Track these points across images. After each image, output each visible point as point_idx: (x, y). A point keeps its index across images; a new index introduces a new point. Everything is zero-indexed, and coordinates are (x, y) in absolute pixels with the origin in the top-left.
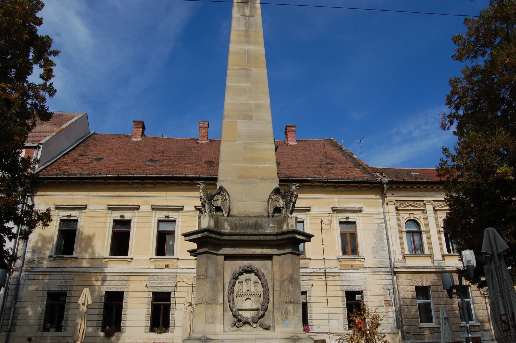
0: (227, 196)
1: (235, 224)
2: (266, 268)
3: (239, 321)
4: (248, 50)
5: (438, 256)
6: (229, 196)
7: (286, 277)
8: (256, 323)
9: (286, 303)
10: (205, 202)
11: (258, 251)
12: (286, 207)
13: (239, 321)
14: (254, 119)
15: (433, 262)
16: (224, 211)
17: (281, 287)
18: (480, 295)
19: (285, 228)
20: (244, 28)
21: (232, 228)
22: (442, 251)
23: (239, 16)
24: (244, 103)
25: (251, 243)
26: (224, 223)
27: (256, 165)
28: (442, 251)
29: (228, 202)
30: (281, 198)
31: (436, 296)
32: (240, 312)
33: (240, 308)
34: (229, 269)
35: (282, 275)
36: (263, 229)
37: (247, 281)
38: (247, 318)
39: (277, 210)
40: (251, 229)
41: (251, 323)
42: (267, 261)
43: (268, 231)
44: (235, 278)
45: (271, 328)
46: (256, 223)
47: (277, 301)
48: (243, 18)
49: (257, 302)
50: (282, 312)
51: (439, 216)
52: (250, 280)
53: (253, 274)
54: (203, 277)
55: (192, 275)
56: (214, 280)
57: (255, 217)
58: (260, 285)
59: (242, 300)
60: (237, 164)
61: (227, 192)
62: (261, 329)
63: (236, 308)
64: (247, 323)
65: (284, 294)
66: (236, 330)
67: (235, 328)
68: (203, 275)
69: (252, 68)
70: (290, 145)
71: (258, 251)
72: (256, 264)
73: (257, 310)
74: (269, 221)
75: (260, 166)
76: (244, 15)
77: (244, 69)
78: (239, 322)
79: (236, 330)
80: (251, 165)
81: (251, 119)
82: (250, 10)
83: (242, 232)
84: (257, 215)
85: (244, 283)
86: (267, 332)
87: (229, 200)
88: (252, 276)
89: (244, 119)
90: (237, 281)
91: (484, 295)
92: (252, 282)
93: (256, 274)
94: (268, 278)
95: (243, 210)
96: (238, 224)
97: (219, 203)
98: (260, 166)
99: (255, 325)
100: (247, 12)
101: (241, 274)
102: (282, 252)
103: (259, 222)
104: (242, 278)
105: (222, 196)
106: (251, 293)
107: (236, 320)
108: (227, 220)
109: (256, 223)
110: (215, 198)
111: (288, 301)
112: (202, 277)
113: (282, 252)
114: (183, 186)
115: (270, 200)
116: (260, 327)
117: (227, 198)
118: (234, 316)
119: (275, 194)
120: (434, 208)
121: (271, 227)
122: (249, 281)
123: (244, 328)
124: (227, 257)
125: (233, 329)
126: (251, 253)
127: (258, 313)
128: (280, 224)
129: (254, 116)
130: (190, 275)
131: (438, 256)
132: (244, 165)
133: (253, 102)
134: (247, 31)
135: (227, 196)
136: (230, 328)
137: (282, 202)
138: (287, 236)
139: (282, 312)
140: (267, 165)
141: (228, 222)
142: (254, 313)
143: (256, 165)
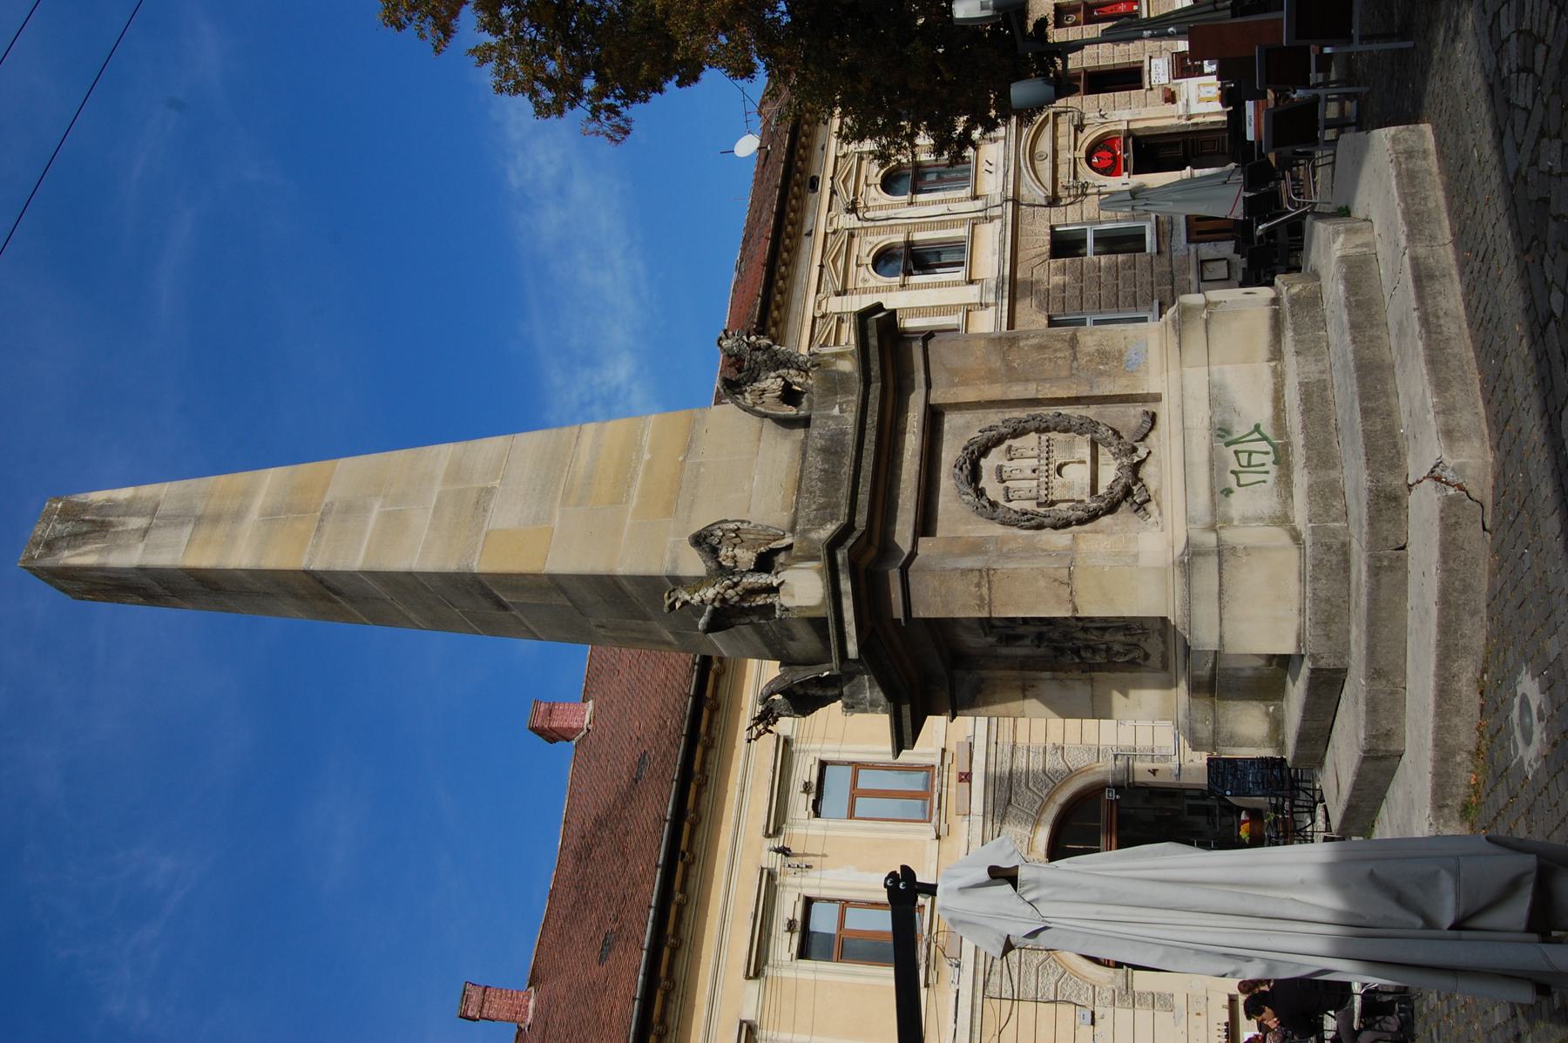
0: (725, 526)
1: (822, 507)
2: (968, 426)
3: (1128, 492)
4: (262, 515)
5: (971, 294)
6: (726, 521)
8: (1134, 450)
9: (1075, 358)
10: (736, 585)
11: (912, 442)
12: (785, 366)
13: (1128, 492)
15: (983, 306)
16: (773, 545)
17: (1027, 380)
18: (1077, 206)
19: (847, 366)
20: (187, 531)
21: (833, 517)
22: (956, 284)
23: (141, 546)
25: (884, 459)
26: (812, 541)
27: (641, 469)
28: (956, 284)
29: (745, 526)
30: (756, 385)
31: (1076, 304)
32: (1102, 490)
35: (992, 377)
36: (844, 433)
39: (789, 395)
40: (841, 465)
41: (1136, 459)
42: (946, 426)
43: (851, 418)
45: (1151, 407)
46: (824, 451)
47: (1069, 388)
48: (154, 536)
49: (1070, 446)
50: (1101, 374)
51: (860, 285)
52: (1000, 469)
53: (983, 462)
54: (984, 582)
55: (979, 1001)
57: (804, 455)
58: (1016, 443)
60: (629, 521)
62: (1152, 435)
63: (1088, 500)
64: (1136, 467)
65: (1048, 366)
66: (1158, 505)
67: (1151, 507)
68: (978, 585)
69: (327, 500)
70: (593, 720)
71: (912, 442)
72: (950, 453)
73: (1094, 445)
74: (822, 416)
75: (647, 456)
76: (145, 532)
77: (322, 520)
78: (1129, 496)
79: (1158, 505)
80: (638, 483)
82: (133, 515)
83: (845, 490)
84: (798, 455)
86: (1162, 420)
87: (743, 522)
89: (485, 510)
90: (1002, 501)
91: (1076, 196)
92: (1007, 463)
93: (984, 451)
94: (995, 418)
95: (779, 497)
96: (822, 500)
97: (746, 557)
98: (647, 456)
99: (1142, 452)
100: (137, 523)
101: (980, 493)
102: (920, 377)
103: (820, 443)
106: (1044, 462)
107: (1124, 505)
108: (805, 531)
109: (824, 451)
112: (985, 591)
113: (920, 377)
114: (671, 1020)
116: (1148, 440)
117: (732, 526)
118: (1112, 509)
119: (742, 393)
120: (838, 294)
121: (841, 411)
123: (1152, 484)
124: (926, 524)
125: (1156, 513)
126: (917, 460)
128: (834, 385)
129: (482, 485)
130: (979, 1008)
131: (971, 294)
132: (634, 502)
133: (437, 488)
134: (199, 520)
135: (725, 526)
137: (769, 381)
138: (873, 342)
139: (1101, 374)
140: (647, 439)
141: (810, 530)
142: (1105, 455)
143: (641, 469)
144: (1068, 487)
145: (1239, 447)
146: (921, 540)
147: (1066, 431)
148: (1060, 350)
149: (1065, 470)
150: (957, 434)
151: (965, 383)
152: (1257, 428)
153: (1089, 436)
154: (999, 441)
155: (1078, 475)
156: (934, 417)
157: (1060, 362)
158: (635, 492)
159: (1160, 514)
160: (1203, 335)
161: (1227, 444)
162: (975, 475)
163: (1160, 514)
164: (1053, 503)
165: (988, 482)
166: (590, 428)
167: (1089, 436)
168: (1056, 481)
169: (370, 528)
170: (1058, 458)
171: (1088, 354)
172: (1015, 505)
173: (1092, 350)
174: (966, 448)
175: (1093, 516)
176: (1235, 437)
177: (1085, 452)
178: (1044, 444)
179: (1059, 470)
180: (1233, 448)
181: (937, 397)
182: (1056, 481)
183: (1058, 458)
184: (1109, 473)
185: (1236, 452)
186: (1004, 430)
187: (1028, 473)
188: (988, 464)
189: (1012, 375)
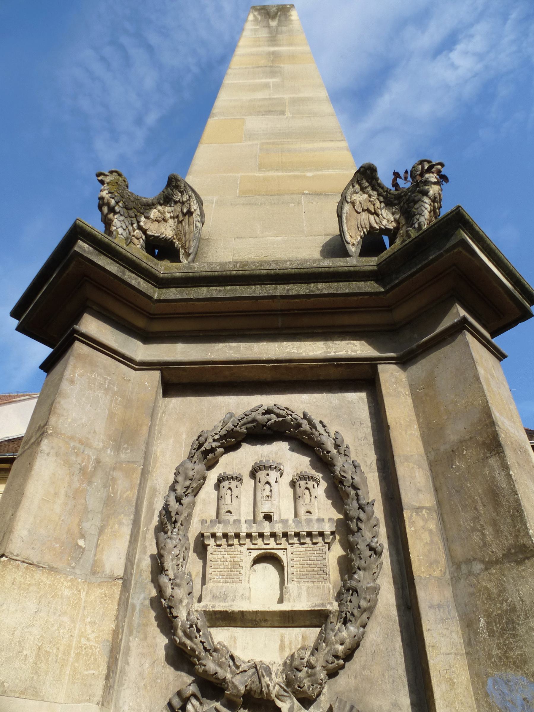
6: (200, 203)
7: (455, 431)
9: (489, 565)
32: (220, 635)
33: (220, 606)
35: (431, 433)
38: (258, 670)
47: (432, 564)
58: (320, 489)
59: (235, 565)
60: (239, 175)
61: (193, 191)
73: (317, 618)
81: (283, 113)
82: (279, 22)
87: (202, 215)
97: (167, 231)
98: (310, 174)
105: (178, 208)
106: (279, 529)
107: (185, 681)
110: (154, 213)
111: (497, 549)
115: (347, 208)
117: (194, 206)
118: (181, 657)
122: (274, 475)
124: (178, 382)
127: (323, 638)
144: (233, 572)
146: (157, 374)
147: (347, 567)
148: (498, 532)
149: (268, 570)
150: (340, 415)
151: (418, 402)
153: (334, 606)
154: (323, 462)
155: (259, 590)
156: (360, 377)
157: (476, 537)
162: (260, 432)
164: (201, 549)
165: (249, 454)
166: (344, 144)
167: (334, 606)
168: (245, 554)
170: (292, 554)
171: (502, 591)
173: (513, 597)
174: (305, 416)
175: (166, 620)
177: (300, 601)
178: (315, 529)
179: (268, 558)
181: (391, 376)
182: (245, 554)
186: (340, 462)
187: (265, 507)
188: (279, 451)
189: (439, 464)
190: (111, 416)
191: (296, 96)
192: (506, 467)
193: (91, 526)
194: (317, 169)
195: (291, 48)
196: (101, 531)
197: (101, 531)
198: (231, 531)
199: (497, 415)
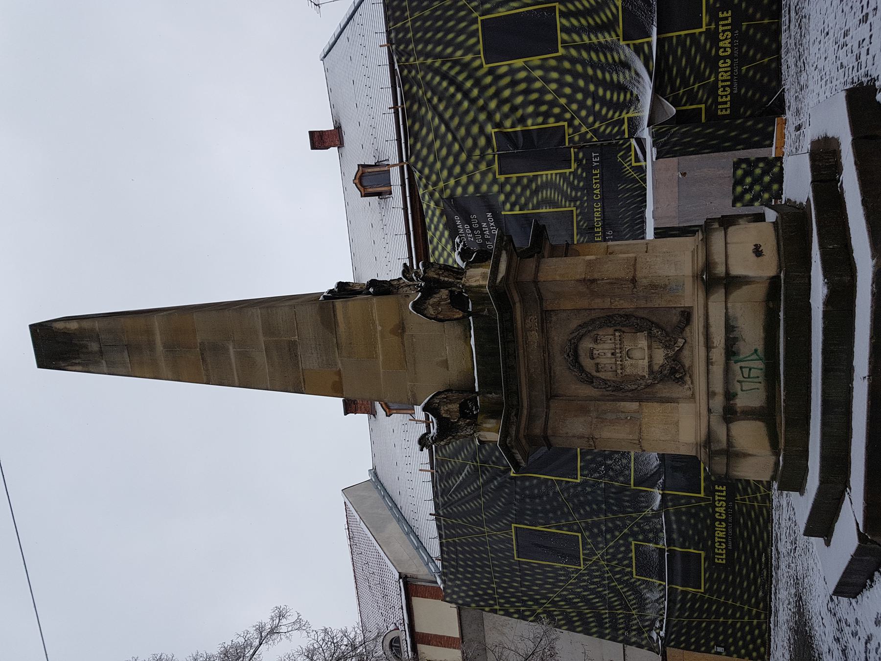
9: (635, 287)
14: (293, 339)
24: (267, 355)
27: (378, 335)
33: (646, 369)
34: (573, 387)
37: (595, 356)
38: (667, 357)
41: (677, 349)
44: (590, 380)
52: (591, 351)
56: (594, 421)
59: (632, 365)
62: (687, 329)
67: (687, 378)
85: (598, 361)
88: (586, 344)
90: (595, 374)
92: (595, 346)
98: (379, 328)
101: (581, 369)
104: (588, 364)
112: (592, 443)
115: (440, 316)
122: (595, 352)
125: (690, 382)
136: (687, 386)
143: (378, 335)
145: (743, 364)
152: (756, 351)
158: (380, 351)
159: (692, 383)
160: (723, 295)
161: (736, 362)
163: (692, 383)
169: (233, 361)
172: (602, 375)
176: (741, 357)
178: (618, 338)
180: (739, 364)
182: (628, 362)
183: (627, 346)
184: (660, 356)
185: (741, 368)
190: (576, 416)
191: (261, 331)
192: (603, 279)
193: (623, 416)
194: (374, 323)
195: (158, 332)
196: (622, 412)
197: (622, 412)
198: (619, 367)
199: (578, 277)
